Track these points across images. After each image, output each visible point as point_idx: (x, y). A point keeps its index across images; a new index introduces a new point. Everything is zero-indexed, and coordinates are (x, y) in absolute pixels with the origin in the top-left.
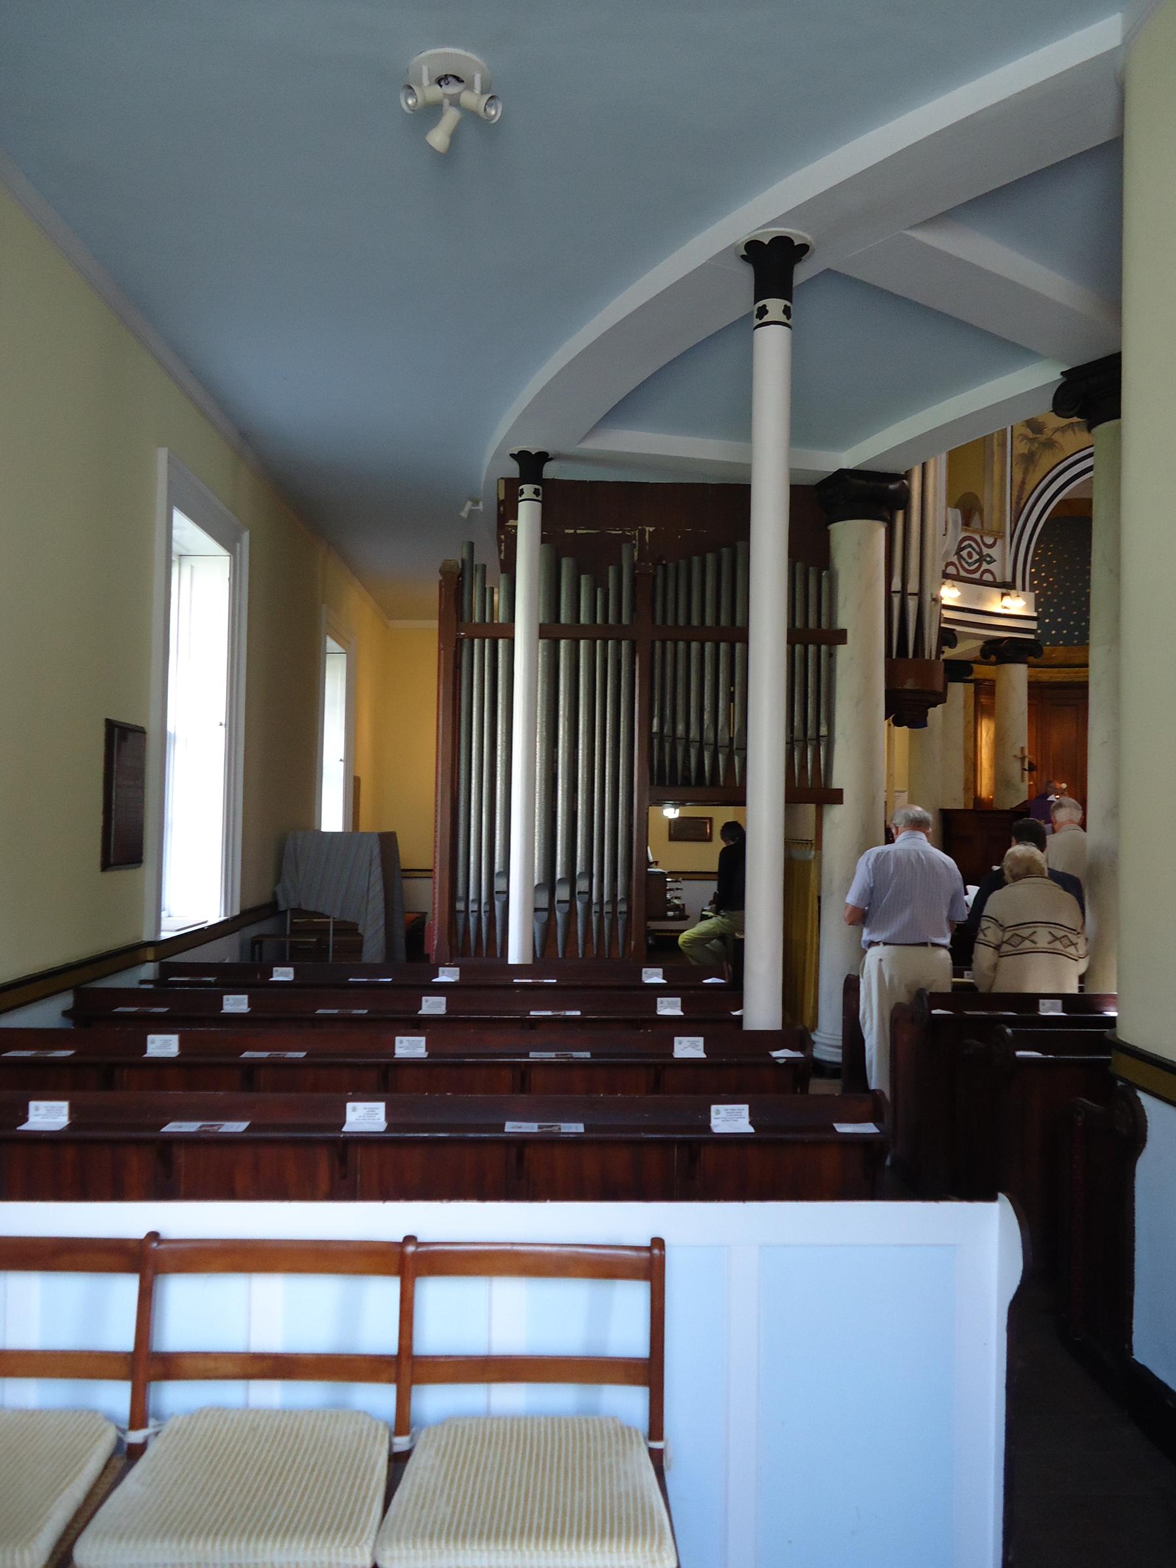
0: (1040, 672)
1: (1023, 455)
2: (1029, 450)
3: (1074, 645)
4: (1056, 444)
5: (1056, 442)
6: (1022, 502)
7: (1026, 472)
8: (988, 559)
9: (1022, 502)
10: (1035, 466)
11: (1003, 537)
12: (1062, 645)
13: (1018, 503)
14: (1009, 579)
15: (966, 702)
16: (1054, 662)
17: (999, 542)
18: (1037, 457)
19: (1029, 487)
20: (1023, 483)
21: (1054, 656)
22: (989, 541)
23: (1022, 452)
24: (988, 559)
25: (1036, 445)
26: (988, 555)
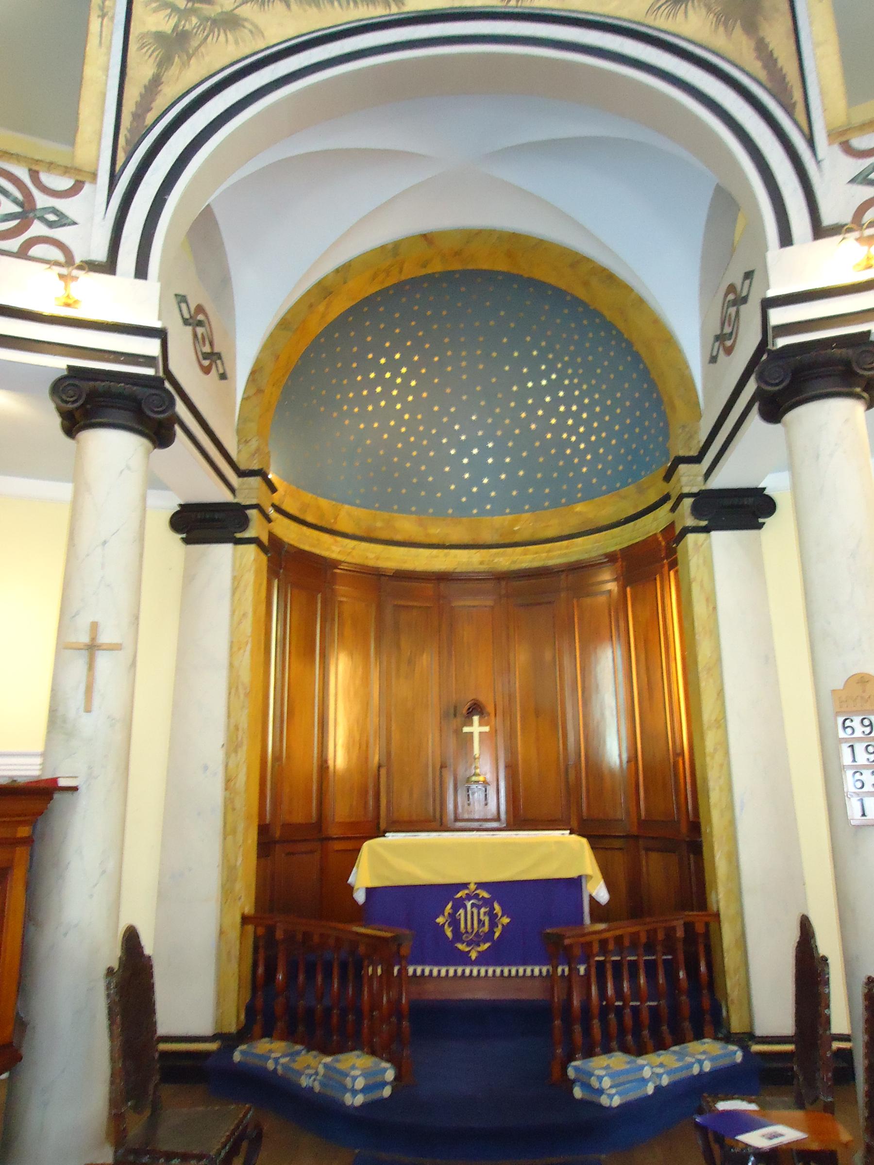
0: (496, 555)
1: (160, 37)
2: (176, 26)
3: (545, 509)
4: (246, 24)
5: (246, 20)
6: (150, 118)
7: (164, 63)
8: (52, 217)
9: (150, 118)
10: (190, 58)
11: (94, 176)
12: (527, 511)
13: (138, 116)
14: (101, 254)
15: (236, 581)
16: (517, 538)
17: (87, 187)
18: (195, 43)
19: (169, 92)
20: (155, 84)
21: (516, 528)
22: (64, 183)
23: (154, 29)
24: (52, 217)
25: (194, 20)
26: (55, 211)
